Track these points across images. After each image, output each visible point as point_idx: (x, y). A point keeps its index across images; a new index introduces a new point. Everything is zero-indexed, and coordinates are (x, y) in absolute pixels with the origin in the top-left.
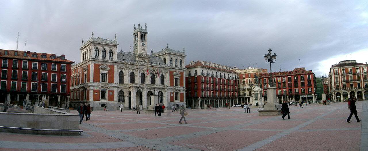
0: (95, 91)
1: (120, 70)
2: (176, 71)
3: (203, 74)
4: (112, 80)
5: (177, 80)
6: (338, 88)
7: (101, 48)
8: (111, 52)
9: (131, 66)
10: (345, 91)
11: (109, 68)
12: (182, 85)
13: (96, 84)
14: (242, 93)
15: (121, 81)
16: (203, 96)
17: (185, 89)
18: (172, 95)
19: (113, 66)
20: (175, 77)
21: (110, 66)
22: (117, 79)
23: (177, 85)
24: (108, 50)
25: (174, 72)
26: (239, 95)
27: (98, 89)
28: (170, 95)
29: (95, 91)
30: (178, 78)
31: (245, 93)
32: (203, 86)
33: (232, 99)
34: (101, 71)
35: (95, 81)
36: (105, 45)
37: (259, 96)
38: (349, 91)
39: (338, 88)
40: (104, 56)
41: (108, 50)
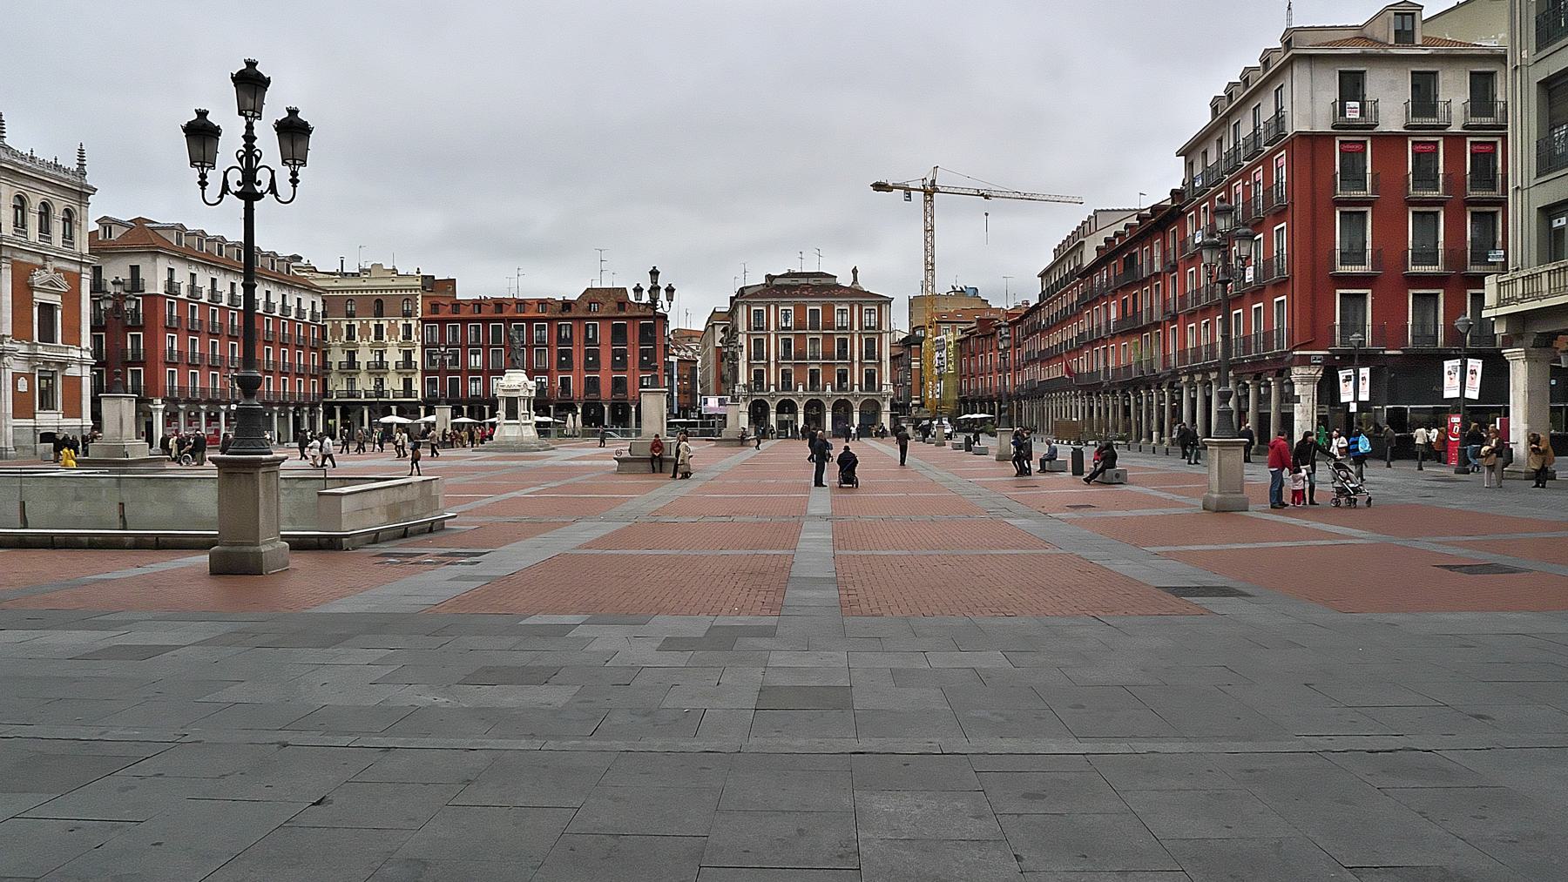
2: (43, 268)
3: (171, 286)
5: (47, 310)
6: (787, 386)
10: (787, 395)
12: (73, 337)
14: (338, 385)
16: (172, 392)
17: (87, 355)
18: (23, 386)
20: (39, 297)
23: (47, 335)
25: (34, 267)
26: (325, 392)
28: (15, 385)
30: (56, 299)
31: (408, 383)
32: (171, 342)
33: (299, 406)
37: (522, 408)
38: (801, 394)
39: (787, 386)
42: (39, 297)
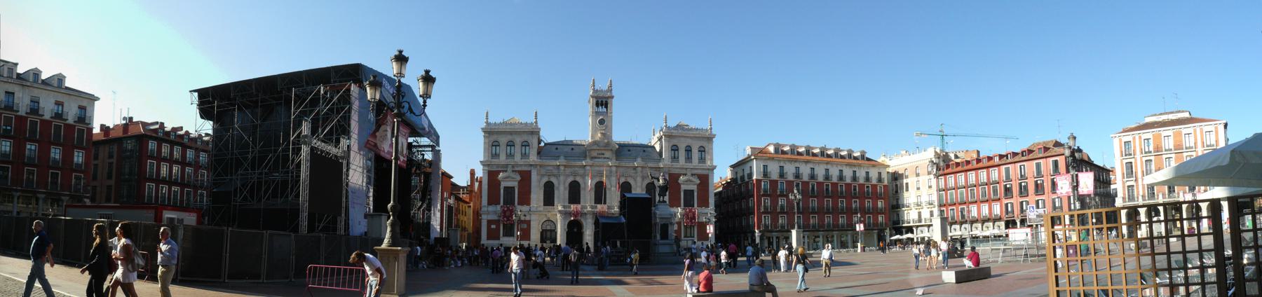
0: (490, 222)
1: (545, 180)
4: (525, 200)
7: (503, 140)
8: (525, 144)
9: (568, 171)
11: (519, 178)
13: (491, 208)
15: (549, 200)
19: (530, 172)
21: (521, 173)
22: (537, 196)
24: (518, 140)
27: (495, 217)
29: (490, 222)
30: (694, 188)
34: (503, 184)
35: (490, 203)
36: (511, 133)
40: (689, 159)
41: (518, 140)
42: (683, 187)
